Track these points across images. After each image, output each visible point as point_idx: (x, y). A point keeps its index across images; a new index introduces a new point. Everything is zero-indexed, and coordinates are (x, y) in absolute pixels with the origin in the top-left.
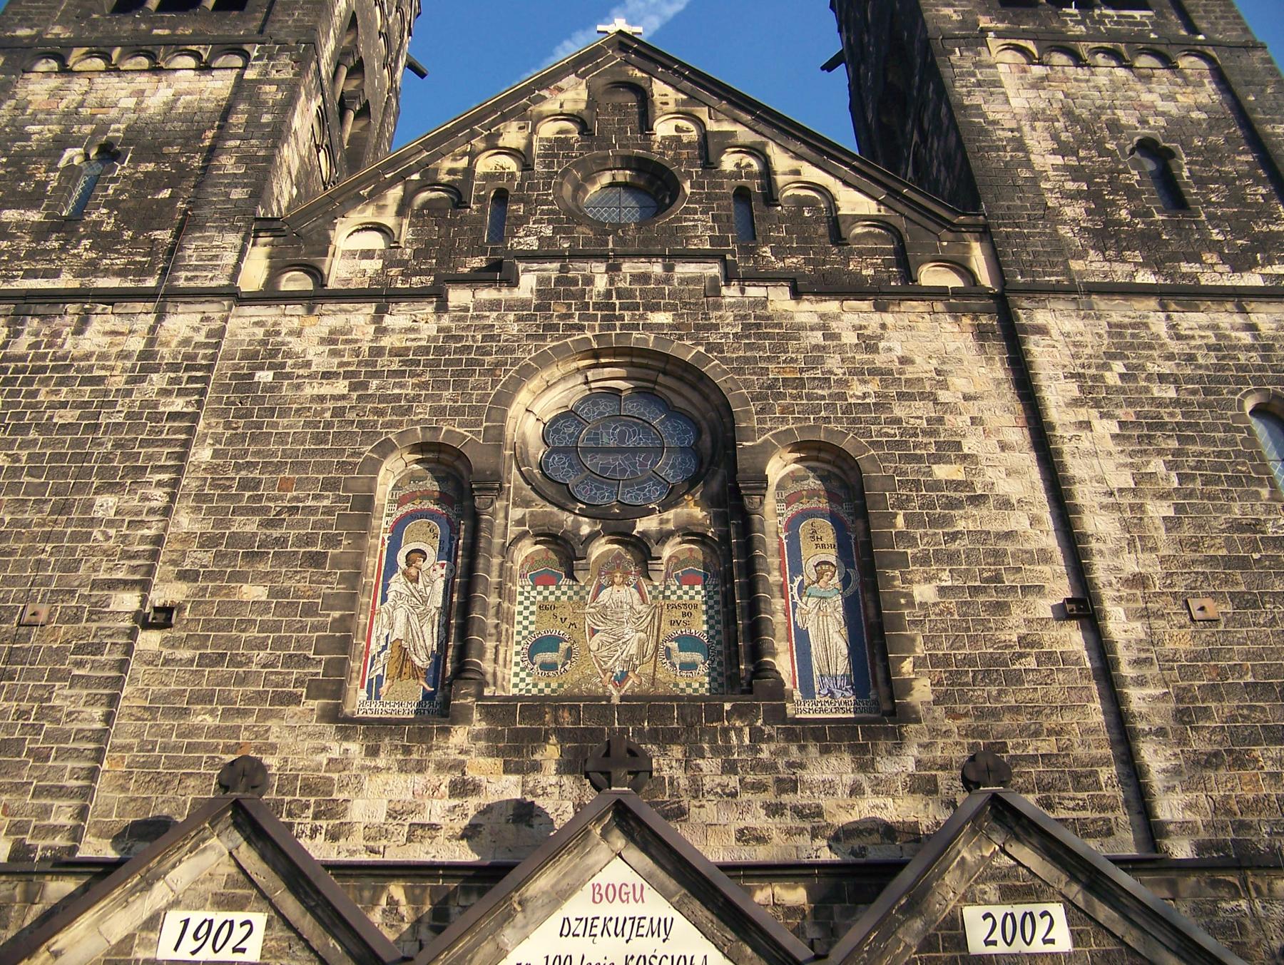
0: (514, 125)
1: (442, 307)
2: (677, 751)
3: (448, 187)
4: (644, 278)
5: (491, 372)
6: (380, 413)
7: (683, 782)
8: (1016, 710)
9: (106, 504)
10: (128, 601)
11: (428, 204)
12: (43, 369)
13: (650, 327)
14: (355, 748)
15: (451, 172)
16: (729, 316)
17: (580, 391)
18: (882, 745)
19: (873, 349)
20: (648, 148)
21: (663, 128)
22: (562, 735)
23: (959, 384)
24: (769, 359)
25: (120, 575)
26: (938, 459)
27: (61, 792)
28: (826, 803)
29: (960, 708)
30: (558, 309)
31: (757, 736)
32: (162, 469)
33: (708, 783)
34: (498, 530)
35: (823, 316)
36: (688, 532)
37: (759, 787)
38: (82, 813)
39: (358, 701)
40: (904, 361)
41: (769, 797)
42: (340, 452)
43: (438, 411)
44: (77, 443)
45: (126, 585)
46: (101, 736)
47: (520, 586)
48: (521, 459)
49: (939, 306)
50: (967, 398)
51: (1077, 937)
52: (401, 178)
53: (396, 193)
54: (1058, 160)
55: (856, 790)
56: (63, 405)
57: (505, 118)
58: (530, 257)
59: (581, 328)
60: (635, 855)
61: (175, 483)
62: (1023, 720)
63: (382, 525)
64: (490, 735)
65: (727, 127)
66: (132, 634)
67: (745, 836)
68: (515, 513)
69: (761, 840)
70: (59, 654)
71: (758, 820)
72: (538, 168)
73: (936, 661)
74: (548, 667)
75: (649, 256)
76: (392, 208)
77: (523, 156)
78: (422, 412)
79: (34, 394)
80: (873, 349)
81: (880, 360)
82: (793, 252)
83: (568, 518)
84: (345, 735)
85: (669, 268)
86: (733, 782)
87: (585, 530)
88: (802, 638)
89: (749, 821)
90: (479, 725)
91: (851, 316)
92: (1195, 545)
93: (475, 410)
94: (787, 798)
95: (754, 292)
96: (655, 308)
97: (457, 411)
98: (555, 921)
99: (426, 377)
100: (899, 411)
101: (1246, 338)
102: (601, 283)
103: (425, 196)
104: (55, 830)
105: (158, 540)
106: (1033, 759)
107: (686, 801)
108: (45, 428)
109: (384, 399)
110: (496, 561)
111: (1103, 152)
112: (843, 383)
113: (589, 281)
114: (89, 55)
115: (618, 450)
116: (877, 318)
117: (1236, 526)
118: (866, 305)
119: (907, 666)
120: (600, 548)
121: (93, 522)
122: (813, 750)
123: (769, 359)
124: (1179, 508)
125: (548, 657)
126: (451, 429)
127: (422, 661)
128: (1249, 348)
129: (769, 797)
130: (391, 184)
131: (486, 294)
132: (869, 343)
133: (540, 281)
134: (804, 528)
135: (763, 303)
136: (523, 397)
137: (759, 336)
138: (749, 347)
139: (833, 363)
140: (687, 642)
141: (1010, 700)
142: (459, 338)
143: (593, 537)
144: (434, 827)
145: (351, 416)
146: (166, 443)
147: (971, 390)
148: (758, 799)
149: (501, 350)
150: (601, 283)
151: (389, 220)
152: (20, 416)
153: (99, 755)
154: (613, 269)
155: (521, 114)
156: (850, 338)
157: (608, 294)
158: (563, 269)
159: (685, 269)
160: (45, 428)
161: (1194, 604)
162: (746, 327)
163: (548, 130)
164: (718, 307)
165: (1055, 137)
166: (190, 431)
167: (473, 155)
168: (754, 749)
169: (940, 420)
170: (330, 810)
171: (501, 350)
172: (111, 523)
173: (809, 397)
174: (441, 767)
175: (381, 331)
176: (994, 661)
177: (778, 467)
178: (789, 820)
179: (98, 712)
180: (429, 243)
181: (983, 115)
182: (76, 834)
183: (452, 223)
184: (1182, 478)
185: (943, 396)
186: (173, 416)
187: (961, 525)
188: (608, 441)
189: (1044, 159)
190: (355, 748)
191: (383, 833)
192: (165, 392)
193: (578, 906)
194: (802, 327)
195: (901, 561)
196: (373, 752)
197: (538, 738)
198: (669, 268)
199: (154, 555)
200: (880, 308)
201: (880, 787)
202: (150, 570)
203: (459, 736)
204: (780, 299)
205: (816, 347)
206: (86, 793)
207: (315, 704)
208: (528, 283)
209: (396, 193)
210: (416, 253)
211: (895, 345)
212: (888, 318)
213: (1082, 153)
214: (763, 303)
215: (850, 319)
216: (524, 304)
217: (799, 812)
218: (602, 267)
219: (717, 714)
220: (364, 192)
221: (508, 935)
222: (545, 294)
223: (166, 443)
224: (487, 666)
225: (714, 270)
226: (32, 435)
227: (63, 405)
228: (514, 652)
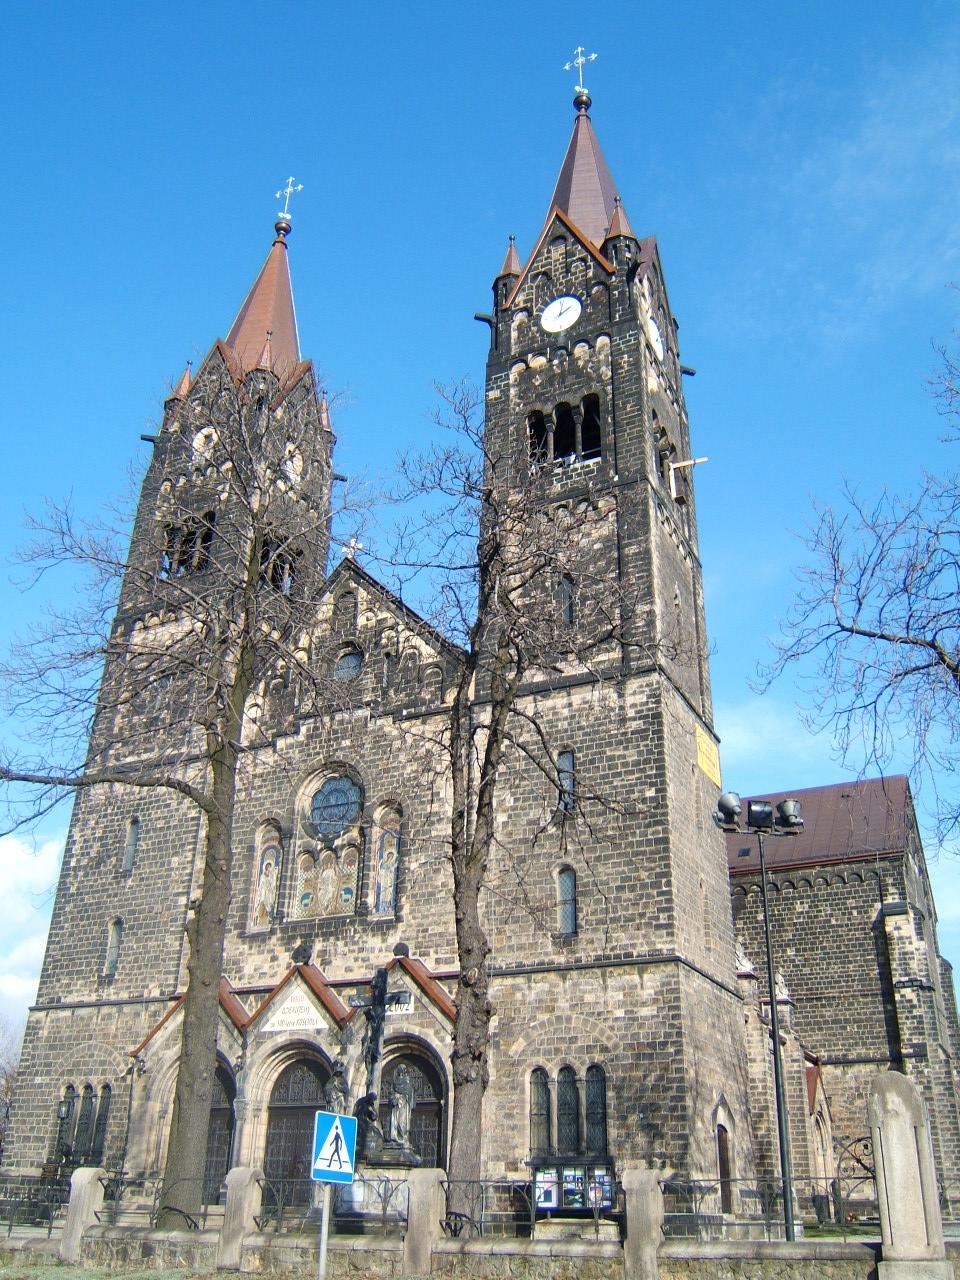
2: (332, 939)
3: (281, 676)
6: (254, 806)
7: (333, 951)
8: (434, 915)
9: (175, 860)
10: (183, 900)
12: (151, 803)
13: (343, 749)
14: (246, 947)
17: (323, 780)
18: (392, 932)
20: (354, 634)
21: (361, 621)
22: (302, 936)
24: (379, 760)
25: (180, 890)
27: (169, 973)
28: (371, 956)
29: (416, 915)
31: (355, 931)
32: (190, 844)
33: (339, 951)
34: (291, 853)
36: (351, 844)
37: (353, 951)
38: (176, 979)
39: (252, 928)
41: (356, 955)
42: (242, 827)
44: (165, 836)
45: (182, 894)
46: (180, 952)
47: (300, 873)
48: (304, 817)
51: (416, 1009)
53: (262, 686)
55: (381, 950)
56: (159, 819)
59: (318, 754)
60: (304, 986)
61: (194, 849)
62: (436, 918)
63: (258, 854)
64: (282, 939)
66: (186, 913)
67: (349, 970)
68: (298, 842)
69: (351, 971)
70: (166, 923)
71: (351, 963)
73: (414, 896)
77: (308, 651)
78: (268, 804)
79: (150, 815)
83: (314, 842)
86: (346, 949)
87: (319, 848)
88: (379, 888)
89: (349, 964)
90: (279, 935)
92: (510, 834)
93: (284, 801)
95: (379, 722)
98: (281, 1009)
99: (269, 788)
101: (566, 712)
104: (169, 985)
105: (191, 874)
106: (435, 935)
107: (333, 958)
108: (155, 830)
109: (257, 799)
110: (290, 866)
111: (544, 589)
112: (404, 767)
114: (152, 616)
115: (337, 805)
117: (530, 823)
118: (419, 722)
119: (403, 899)
120: (323, 855)
121: (172, 869)
122: (370, 934)
123: (379, 760)
124: (510, 817)
125: (306, 901)
126: (280, 812)
127: (268, 909)
128: (565, 719)
129: (356, 955)
131: (290, 740)
133: (308, 730)
135: (381, 728)
136: (301, 790)
138: (374, 754)
140: (348, 891)
141: (433, 911)
143: (321, 850)
144: (265, 974)
145: (246, 810)
146: (190, 832)
148: (352, 956)
151: (260, 701)
152: (147, 825)
153: (179, 958)
160: (155, 830)
161: (502, 864)
163: (318, 632)
166: (198, 825)
168: (354, 937)
170: (239, 970)
172: (177, 869)
173: (392, 776)
174: (269, 952)
175: (256, 765)
176: (432, 894)
177: (378, 814)
178: (360, 963)
179: (177, 943)
182: (175, 986)
183: (282, 697)
184: (516, 800)
186: (193, 819)
187: (434, 833)
188: (333, 801)
190: (246, 947)
191: (252, 977)
192: (189, 808)
193: (288, 1004)
196: (251, 948)
199: (190, 880)
200: (424, 723)
202: (189, 887)
203: (274, 939)
204: (387, 725)
206: (177, 972)
207: (236, 932)
208: (303, 730)
209: (262, 686)
214: (381, 728)
216: (301, 744)
217: (363, 960)
219: (344, 924)
221: (270, 1014)
222: (309, 737)
223: (190, 832)
224: (285, 910)
226: (152, 834)
227: (159, 819)
228: (296, 902)
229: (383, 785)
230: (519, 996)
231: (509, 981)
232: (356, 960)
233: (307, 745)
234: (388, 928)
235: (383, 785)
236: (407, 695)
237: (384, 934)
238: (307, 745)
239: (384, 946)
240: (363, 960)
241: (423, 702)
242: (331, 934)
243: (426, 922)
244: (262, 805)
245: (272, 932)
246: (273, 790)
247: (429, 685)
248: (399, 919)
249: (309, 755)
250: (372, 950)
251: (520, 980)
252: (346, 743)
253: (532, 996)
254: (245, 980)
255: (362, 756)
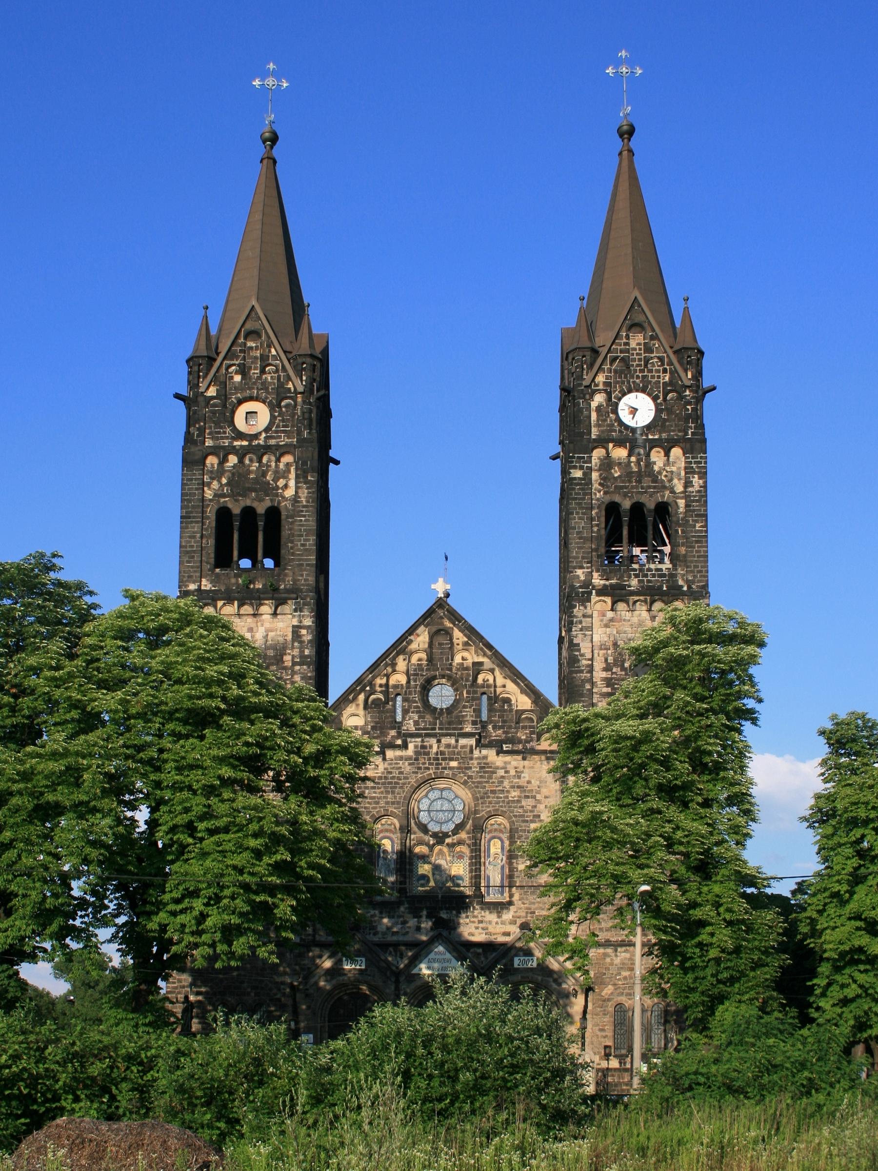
0: (401, 657)
1: (384, 759)
4: (448, 746)
5: (401, 787)
11: (374, 700)
13: (451, 768)
14: (377, 912)
15: (381, 686)
16: (475, 762)
19: (519, 777)
20: (451, 670)
21: (458, 659)
23: (545, 791)
26: (532, 821)
28: (490, 927)
30: (421, 761)
35: (505, 763)
40: (529, 782)
43: (387, 803)
49: (543, 757)
50: (546, 797)
52: (363, 689)
53: (362, 697)
54: (604, 675)
57: (398, 654)
58: (412, 736)
59: (428, 769)
65: (481, 659)
72: (412, 683)
74: (423, 885)
75: (450, 735)
76: (362, 706)
78: (382, 803)
80: (519, 777)
81: (522, 782)
82: (500, 728)
84: (374, 909)
85: (457, 741)
91: (515, 761)
93: (398, 803)
94: (481, 925)
95: (484, 752)
96: (451, 759)
97: (393, 803)
100: (523, 803)
102: (435, 749)
103: (373, 697)
109: (372, 798)
111: (623, 668)
112: (508, 792)
113: (431, 747)
116: (522, 763)
118: (520, 757)
130: (359, 694)
131: (398, 753)
132: (518, 775)
133: (416, 747)
134: (492, 842)
135: (485, 757)
137: (485, 772)
138: (481, 777)
139: (506, 783)
142: (391, 773)
147: (547, 794)
148: (473, 925)
149: (405, 778)
150: (435, 749)
154: (439, 741)
155: (403, 651)
156: (513, 772)
157: (437, 754)
158: (423, 741)
159: (463, 741)
162: (481, 768)
164: (471, 759)
165: (606, 660)
167: (388, 676)
169: (535, 807)
170: (374, 928)
171: (405, 778)
178: (480, 930)
180: (376, 723)
181: (579, 650)
183: (383, 712)
185: (538, 797)
189: (599, 674)
194: (498, 768)
195: (516, 857)
197: (421, 909)
198: (457, 741)
200: (524, 759)
201: (503, 923)
203: (402, 909)
205: (502, 777)
208: (411, 746)
209: (362, 697)
210: (373, 728)
211: (526, 776)
212: (526, 763)
213: (614, 670)
215: (514, 763)
216: (410, 758)
217: (483, 929)
218: (433, 741)
220: (351, 697)
225: (472, 741)
229: (490, 803)
230: (608, 960)
231: (601, 950)
232: (477, 928)
233: (417, 759)
234: (502, 909)
235: (490, 803)
236: (504, 732)
237: (498, 913)
238: (417, 759)
239: (499, 920)
240: (483, 929)
241: (520, 741)
242: (454, 909)
243: (533, 906)
244: (378, 803)
245: (399, 903)
246: (387, 792)
247: (524, 728)
248: (510, 903)
249: (419, 768)
250: (490, 922)
251: (609, 951)
252: (454, 764)
253: (617, 961)
254: (380, 935)
255: (470, 777)
